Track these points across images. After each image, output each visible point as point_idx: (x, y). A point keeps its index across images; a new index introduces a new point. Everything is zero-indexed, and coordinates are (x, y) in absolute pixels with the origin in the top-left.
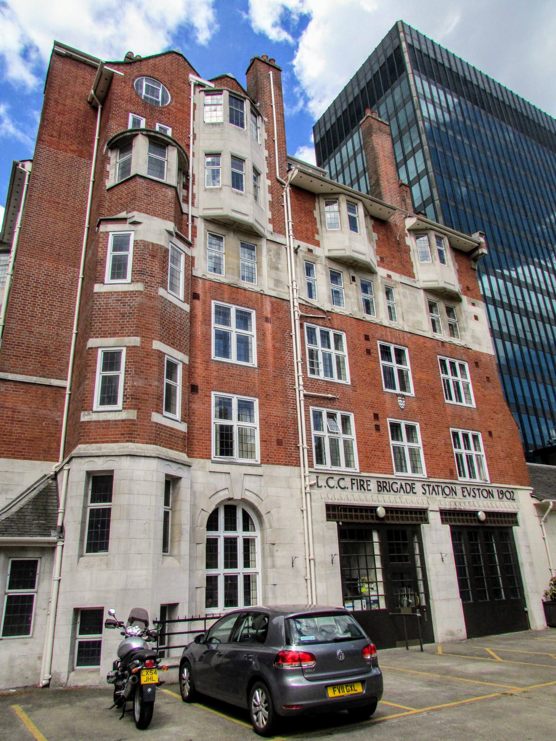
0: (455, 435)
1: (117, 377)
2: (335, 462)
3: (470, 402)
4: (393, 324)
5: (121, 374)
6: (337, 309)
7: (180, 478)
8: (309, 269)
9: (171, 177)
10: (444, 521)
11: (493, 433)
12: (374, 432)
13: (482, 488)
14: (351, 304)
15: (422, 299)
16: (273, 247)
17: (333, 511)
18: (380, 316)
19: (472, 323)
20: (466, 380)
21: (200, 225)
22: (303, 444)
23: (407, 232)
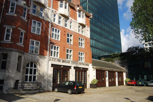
0: (79, 53)
1: (10, 34)
2: (54, 56)
3: (83, 46)
4: (70, 29)
6: (59, 25)
7: (22, 56)
8: (55, 15)
10: (74, 69)
12: (63, 51)
14: (62, 24)
15: (78, 25)
17: (52, 65)
18: (68, 27)
19: (87, 31)
20: (83, 42)
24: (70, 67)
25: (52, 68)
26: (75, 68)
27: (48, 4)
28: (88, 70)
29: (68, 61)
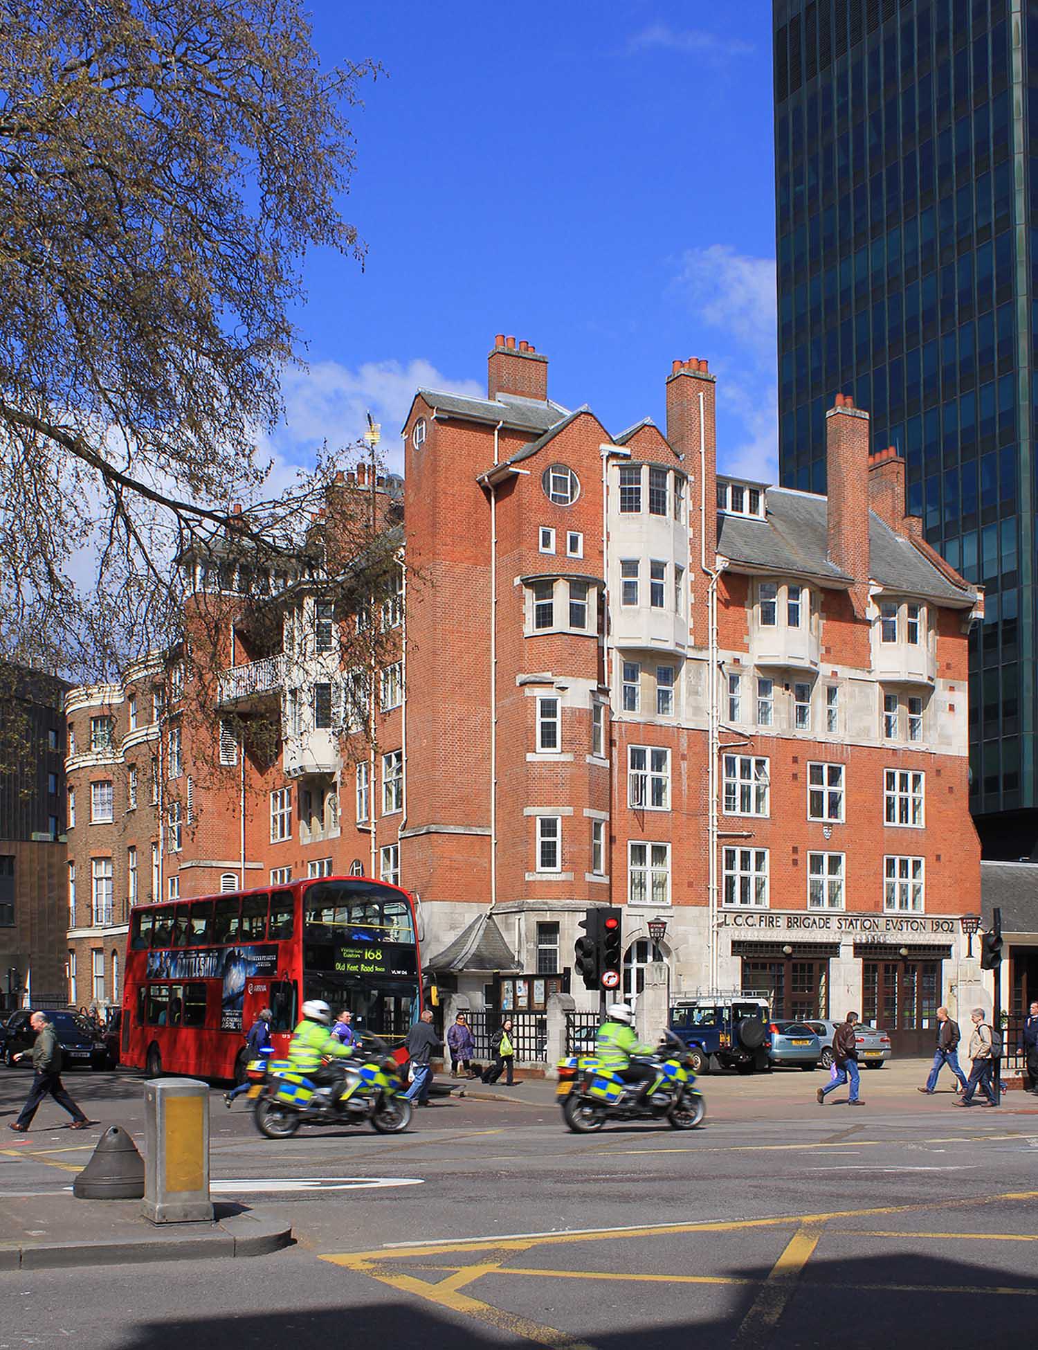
2: (744, 899)
5: (558, 839)
8: (734, 680)
9: (591, 628)
10: (856, 955)
11: (942, 858)
14: (779, 722)
15: (876, 695)
16: (693, 664)
17: (738, 947)
18: (815, 729)
19: (944, 717)
22: (713, 885)
23: (870, 599)
25: (738, 960)
26: (859, 949)
27: (693, 632)
28: (949, 956)
29: (817, 918)
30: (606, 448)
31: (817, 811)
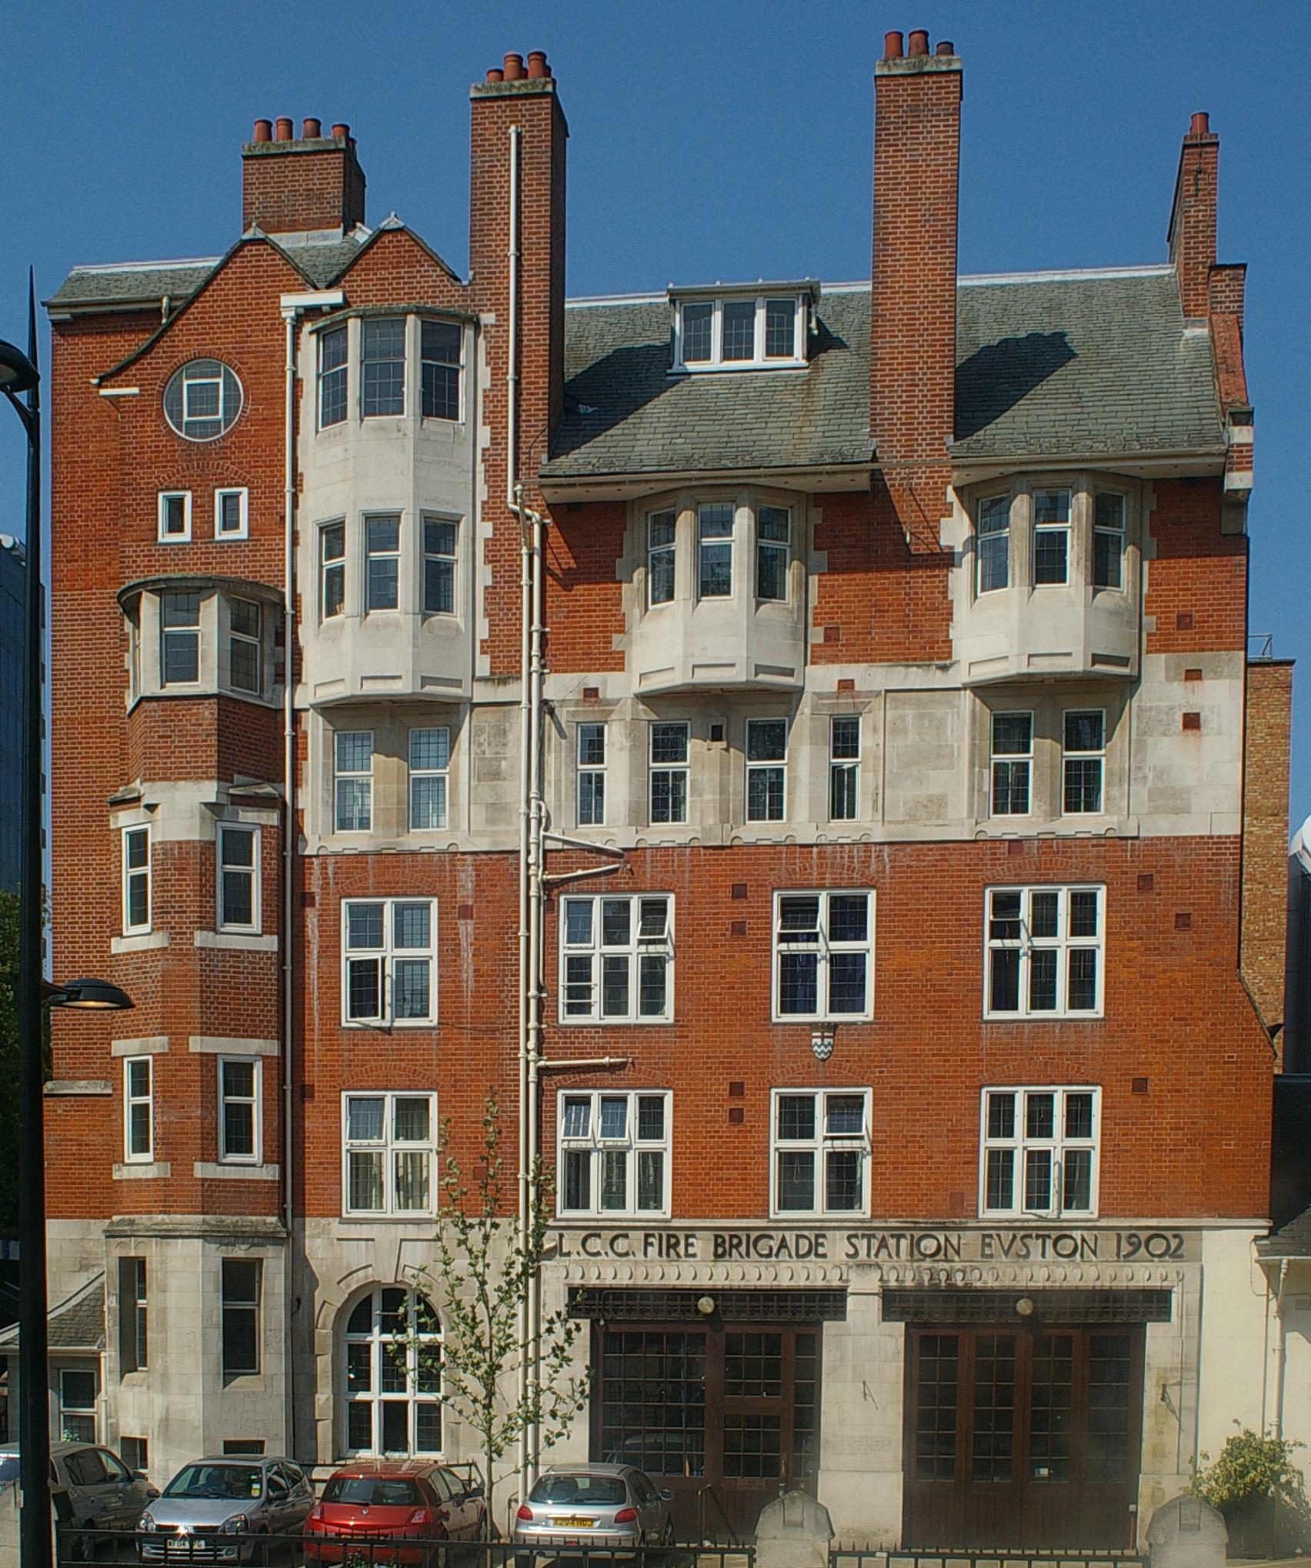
12: (725, 1127)
13: (1054, 1234)
15: (962, 723)
21: (315, 727)
24: (830, 1302)
27: (488, 647)
29: (791, 1237)
30: (291, 302)
31: (798, 996)
